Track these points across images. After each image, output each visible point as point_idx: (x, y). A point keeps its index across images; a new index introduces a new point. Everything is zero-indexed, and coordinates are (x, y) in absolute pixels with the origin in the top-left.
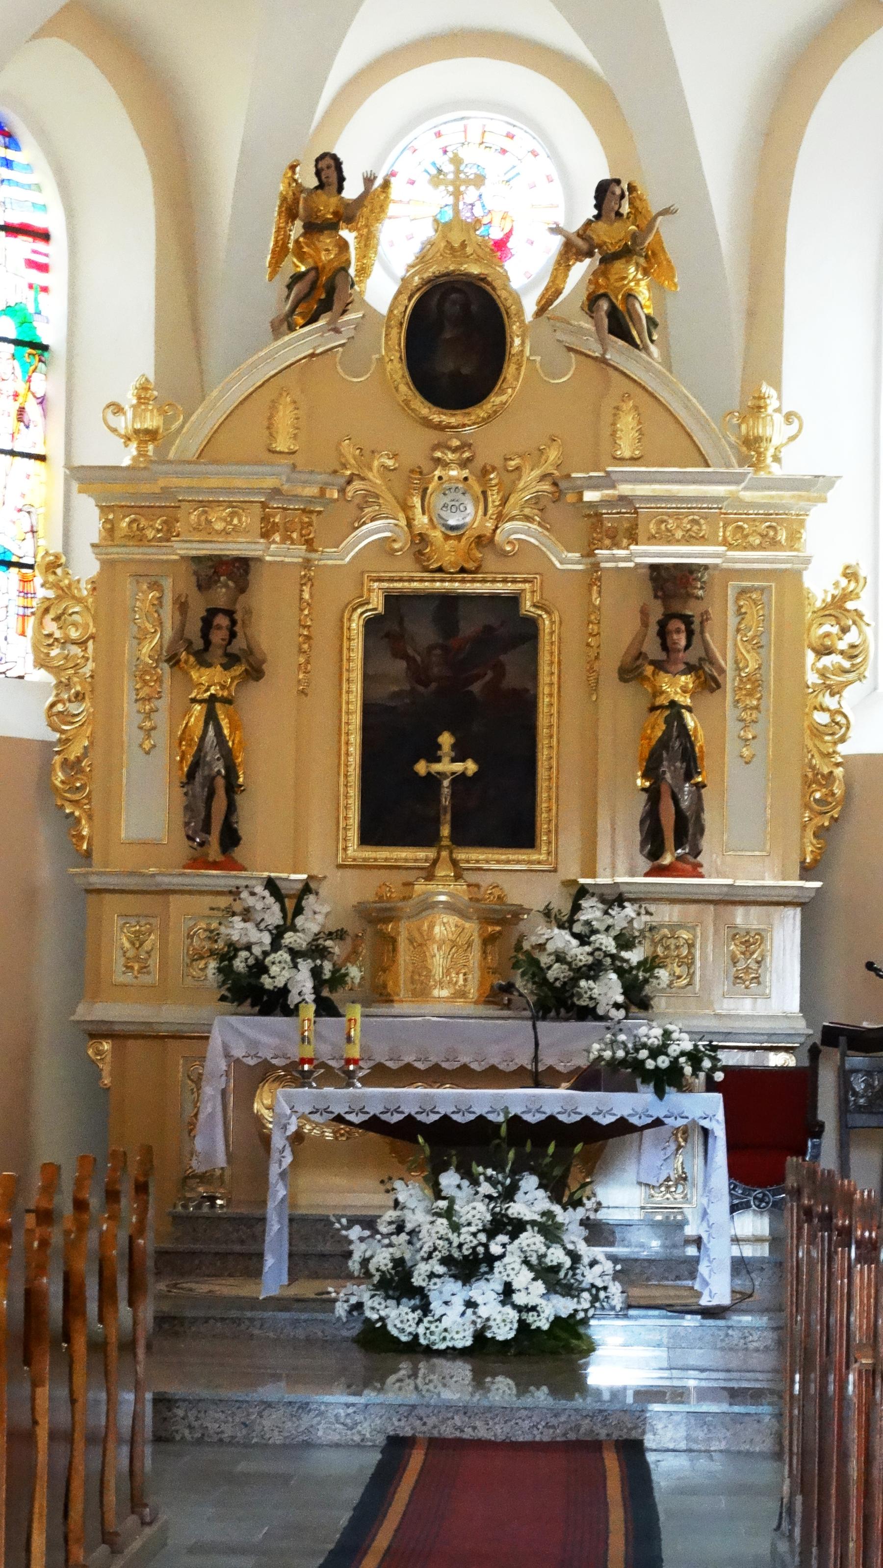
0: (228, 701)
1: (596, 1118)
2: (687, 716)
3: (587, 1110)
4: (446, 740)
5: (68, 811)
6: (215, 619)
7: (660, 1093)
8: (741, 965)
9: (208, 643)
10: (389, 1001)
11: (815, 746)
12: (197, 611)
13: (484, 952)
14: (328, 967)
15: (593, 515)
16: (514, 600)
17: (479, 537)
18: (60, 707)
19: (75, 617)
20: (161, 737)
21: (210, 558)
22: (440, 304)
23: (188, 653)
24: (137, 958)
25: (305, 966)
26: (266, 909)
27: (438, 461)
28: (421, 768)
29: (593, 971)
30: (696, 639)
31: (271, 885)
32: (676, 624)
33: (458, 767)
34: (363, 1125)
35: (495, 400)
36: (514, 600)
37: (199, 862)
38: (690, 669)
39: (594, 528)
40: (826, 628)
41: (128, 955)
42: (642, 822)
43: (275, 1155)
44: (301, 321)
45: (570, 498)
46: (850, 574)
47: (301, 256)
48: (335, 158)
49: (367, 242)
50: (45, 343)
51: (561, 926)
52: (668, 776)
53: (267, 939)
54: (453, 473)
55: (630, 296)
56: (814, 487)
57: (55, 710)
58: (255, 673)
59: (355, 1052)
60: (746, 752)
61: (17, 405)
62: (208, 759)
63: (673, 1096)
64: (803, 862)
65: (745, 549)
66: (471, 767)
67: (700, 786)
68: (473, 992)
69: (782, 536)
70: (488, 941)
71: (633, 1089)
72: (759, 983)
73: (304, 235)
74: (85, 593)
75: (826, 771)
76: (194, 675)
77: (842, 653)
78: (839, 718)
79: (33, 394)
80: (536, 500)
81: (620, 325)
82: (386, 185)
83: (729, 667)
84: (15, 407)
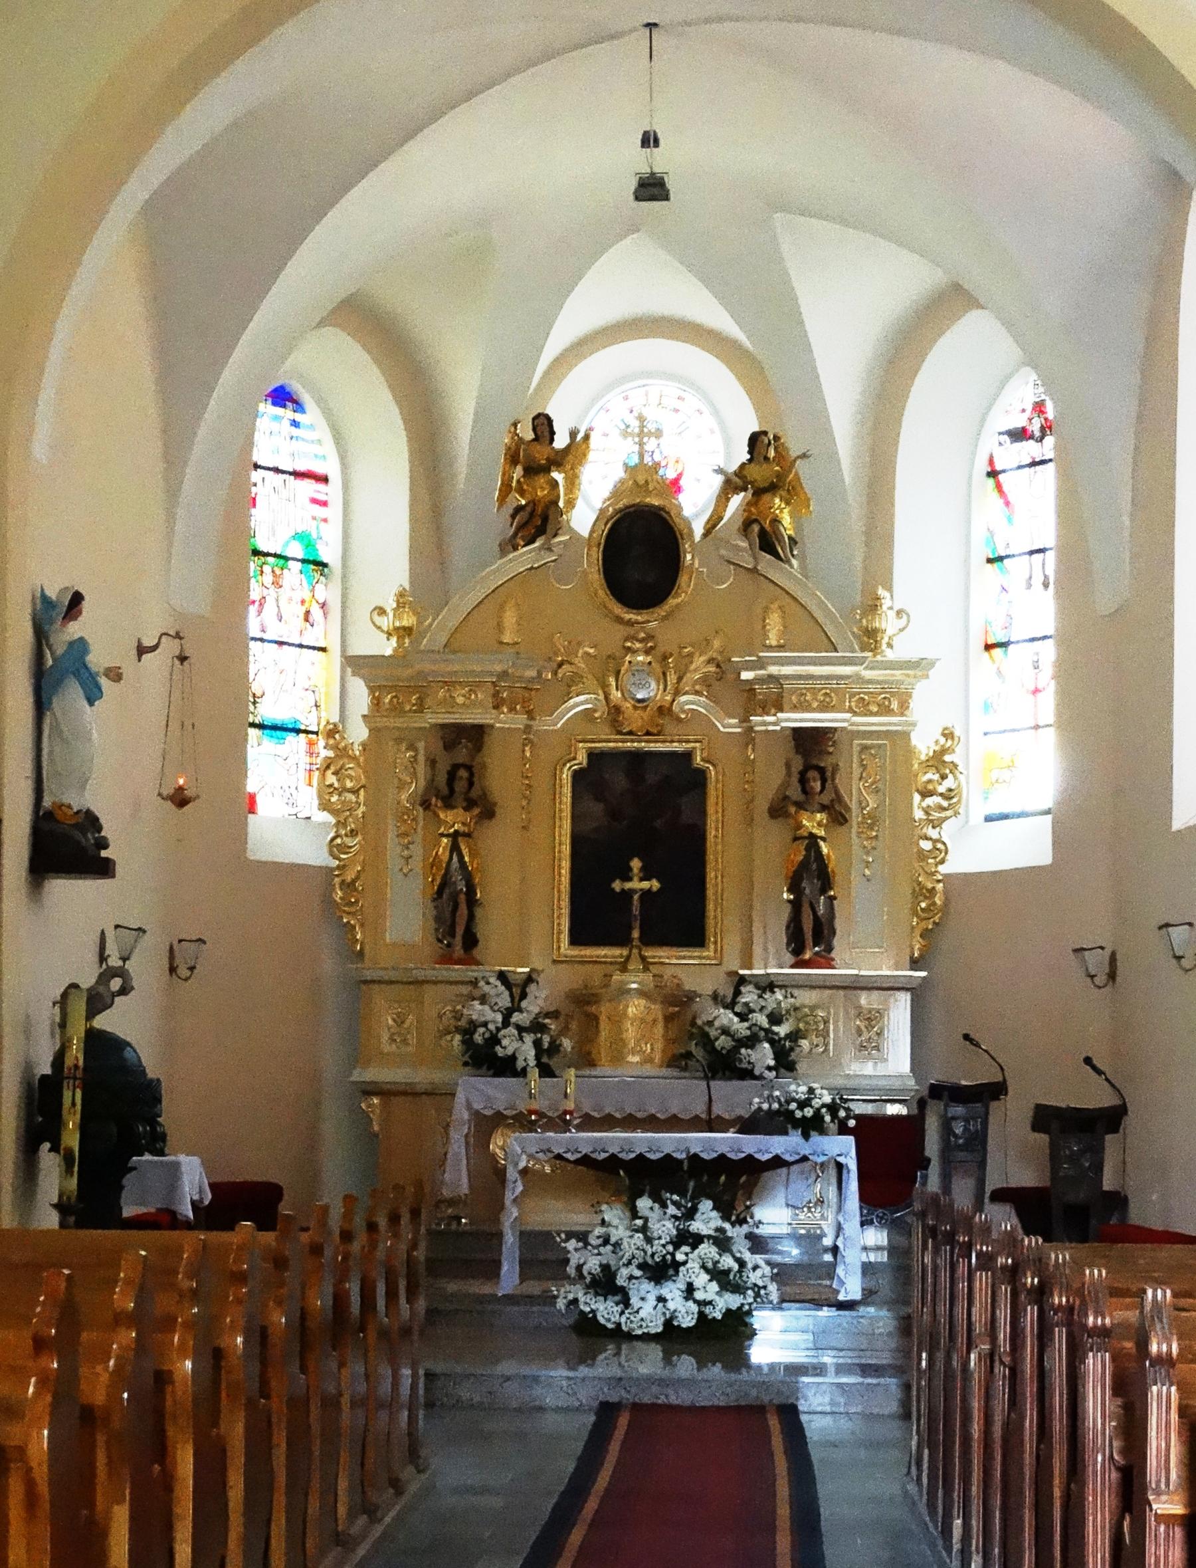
0: (468, 835)
1: (756, 1156)
2: (822, 843)
3: (749, 1150)
4: (636, 864)
6: (457, 772)
7: (806, 1136)
9: (452, 791)
10: (592, 1064)
12: (443, 768)
13: (666, 1027)
14: (546, 1040)
15: (749, 689)
16: (688, 756)
17: (661, 707)
18: (339, 841)
19: (350, 772)
20: (417, 864)
24: (399, 1034)
25: (529, 1039)
26: (498, 995)
27: (629, 649)
28: (617, 885)
29: (751, 1041)
31: (502, 976)
32: (812, 774)
33: (645, 885)
34: (577, 1162)
35: (672, 602)
36: (688, 756)
38: (823, 808)
39: (749, 699)
40: (929, 776)
42: (788, 927)
43: (510, 1185)
44: (522, 543)
45: (730, 676)
46: (948, 734)
47: (522, 492)
49: (572, 482)
51: (726, 1007)
52: (807, 891)
53: (499, 1018)
54: (640, 658)
55: (776, 521)
56: (920, 666)
58: (489, 813)
59: (570, 1105)
60: (867, 872)
61: (303, 609)
63: (815, 1138)
64: (911, 958)
65: (866, 715)
66: (655, 885)
68: (657, 1058)
69: (895, 705)
70: (668, 1019)
71: (786, 1133)
73: (524, 476)
74: (357, 753)
75: (930, 886)
76: (442, 816)
77: (941, 795)
78: (939, 846)
80: (705, 681)
81: (768, 542)
82: (587, 437)
83: (854, 806)
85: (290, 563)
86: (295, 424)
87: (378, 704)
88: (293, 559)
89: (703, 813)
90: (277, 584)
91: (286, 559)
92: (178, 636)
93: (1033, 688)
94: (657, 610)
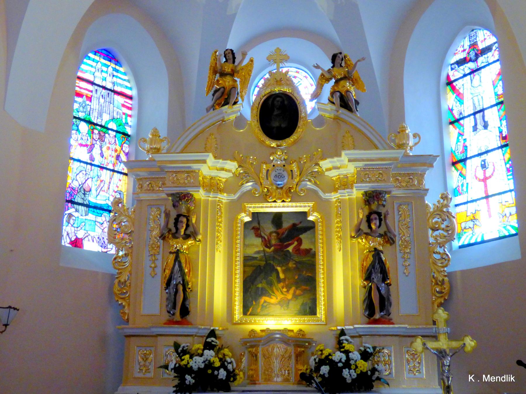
2: (382, 254)
5: (120, 303)
8: (412, 365)
9: (177, 229)
10: (255, 384)
11: (435, 268)
20: (159, 270)
21: (178, 193)
22: (273, 102)
23: (169, 234)
24: (145, 366)
30: (383, 222)
37: (171, 322)
38: (380, 236)
40: (436, 219)
41: (141, 364)
48: (233, 54)
50: (129, 134)
57: (116, 260)
62: (175, 277)
67: (389, 284)
68: (292, 378)
72: (420, 373)
75: (441, 279)
77: (443, 229)
79: (124, 151)
84: (115, 154)
85: (110, 132)
86: (117, 71)
87: (142, 188)
88: (112, 130)
89: (314, 242)
90: (102, 138)
91: (108, 129)
93: (482, 177)
94: (287, 140)
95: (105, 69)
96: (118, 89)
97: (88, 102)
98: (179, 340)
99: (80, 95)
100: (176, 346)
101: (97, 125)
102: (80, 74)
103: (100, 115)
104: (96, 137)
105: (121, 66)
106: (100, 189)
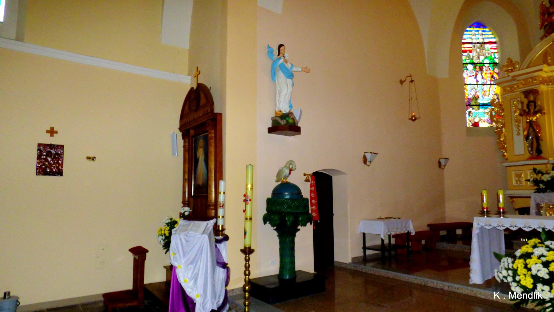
9: (529, 110)
20: (521, 132)
37: (531, 158)
84: (490, 76)
90: (481, 69)
91: (484, 64)
92: (410, 76)
95: (477, 33)
96: (486, 41)
97: (470, 54)
98: (536, 167)
99: (465, 51)
100: (535, 170)
101: (477, 63)
102: (463, 41)
103: (478, 58)
104: (478, 69)
105: (486, 28)
106: (484, 95)
